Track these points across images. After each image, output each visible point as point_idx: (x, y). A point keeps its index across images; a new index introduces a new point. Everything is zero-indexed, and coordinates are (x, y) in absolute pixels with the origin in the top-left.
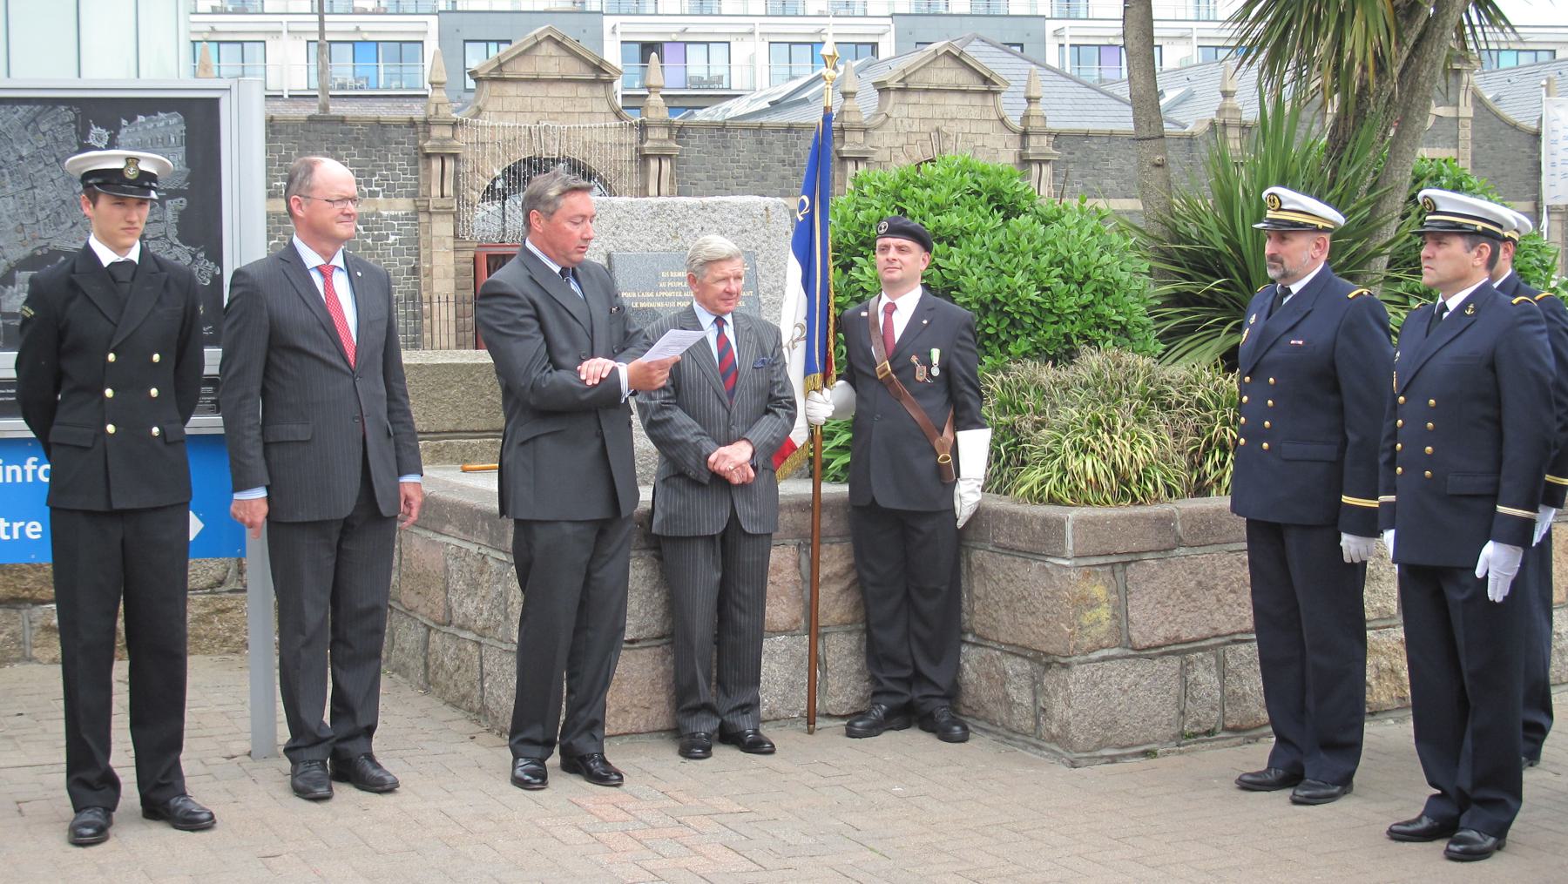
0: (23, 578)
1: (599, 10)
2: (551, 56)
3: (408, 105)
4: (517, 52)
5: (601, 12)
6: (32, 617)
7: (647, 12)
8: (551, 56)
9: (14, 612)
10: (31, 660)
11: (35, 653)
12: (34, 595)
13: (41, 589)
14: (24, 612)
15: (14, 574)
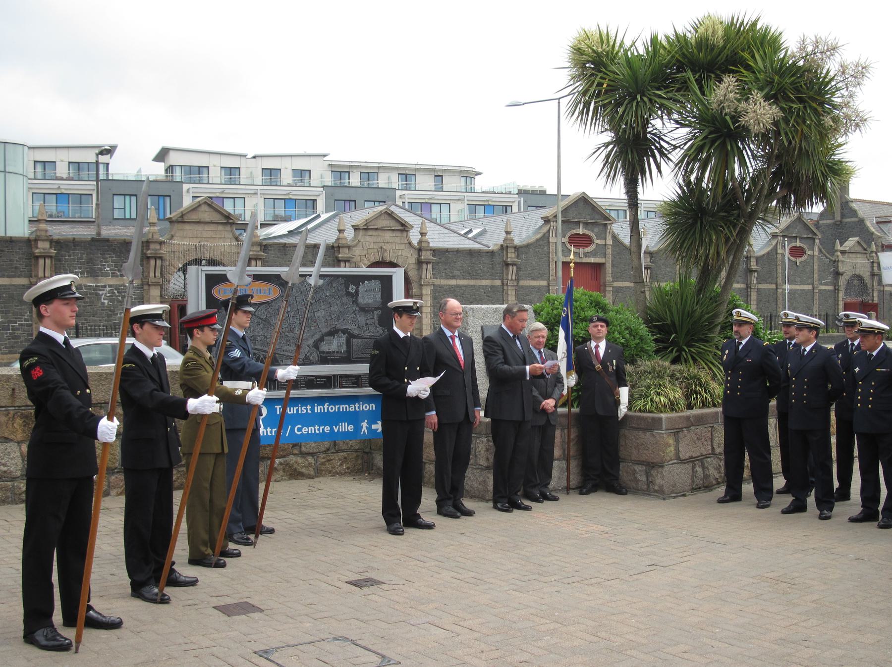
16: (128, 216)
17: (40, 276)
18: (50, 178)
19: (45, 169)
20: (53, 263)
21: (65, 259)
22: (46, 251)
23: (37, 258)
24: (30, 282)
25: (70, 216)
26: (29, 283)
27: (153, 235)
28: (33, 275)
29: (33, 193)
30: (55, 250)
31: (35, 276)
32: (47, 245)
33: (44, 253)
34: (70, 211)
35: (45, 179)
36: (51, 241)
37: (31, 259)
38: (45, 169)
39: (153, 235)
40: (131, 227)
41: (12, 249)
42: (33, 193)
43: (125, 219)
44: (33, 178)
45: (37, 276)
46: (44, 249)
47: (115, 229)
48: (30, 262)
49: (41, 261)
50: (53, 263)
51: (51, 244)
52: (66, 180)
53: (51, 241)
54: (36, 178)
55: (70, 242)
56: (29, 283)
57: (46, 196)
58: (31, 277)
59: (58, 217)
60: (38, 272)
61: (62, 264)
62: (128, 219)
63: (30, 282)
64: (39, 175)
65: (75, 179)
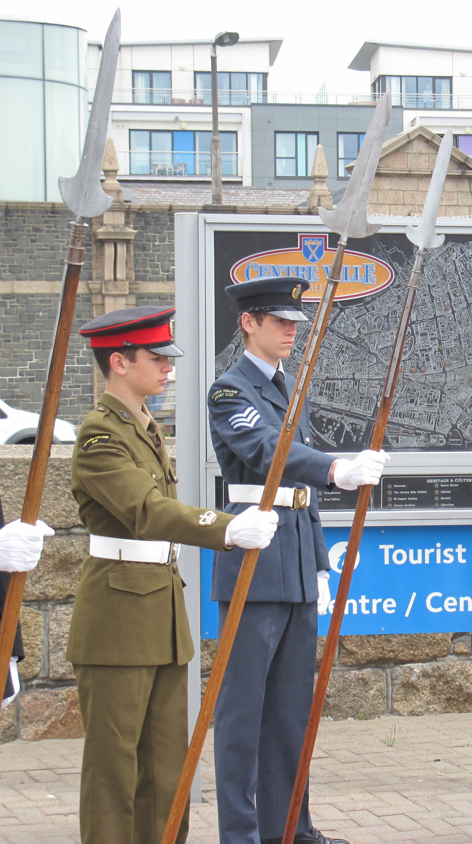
0: (389, 641)
1: (398, 104)
2: (421, 154)
3: (233, 191)
4: (391, 150)
5: (401, 107)
6: (394, 676)
7: (443, 107)
8: (421, 154)
9: (380, 671)
10: (394, 712)
11: (396, 705)
12: (396, 656)
13: (403, 651)
14: (388, 671)
15: (383, 638)
16: (302, 173)
17: (106, 279)
18: (161, 101)
19: (151, 86)
20: (132, 253)
21: (154, 246)
22: (118, 230)
23: (102, 243)
24: (90, 290)
25: (198, 173)
26: (87, 291)
27: (319, 201)
28: (94, 277)
29: (130, 130)
30: (135, 228)
31: (98, 278)
32: (120, 218)
33: (115, 233)
34: (197, 163)
35: (152, 104)
36: (128, 212)
37: (90, 245)
38: (151, 86)
39: (319, 201)
40: (303, 192)
41: (55, 227)
42: (130, 130)
43: (297, 178)
44: (131, 102)
45: (101, 277)
46: (113, 227)
47: (273, 195)
48: (89, 251)
49: (109, 250)
50: (132, 253)
51: (127, 217)
52: (190, 105)
53: (128, 212)
54: (136, 101)
55: (163, 213)
56: (87, 291)
57: (154, 135)
58: (90, 279)
59: (175, 174)
60: (103, 270)
61: (148, 255)
62: (302, 178)
63: (90, 290)
64: (142, 97)
65: (205, 103)
